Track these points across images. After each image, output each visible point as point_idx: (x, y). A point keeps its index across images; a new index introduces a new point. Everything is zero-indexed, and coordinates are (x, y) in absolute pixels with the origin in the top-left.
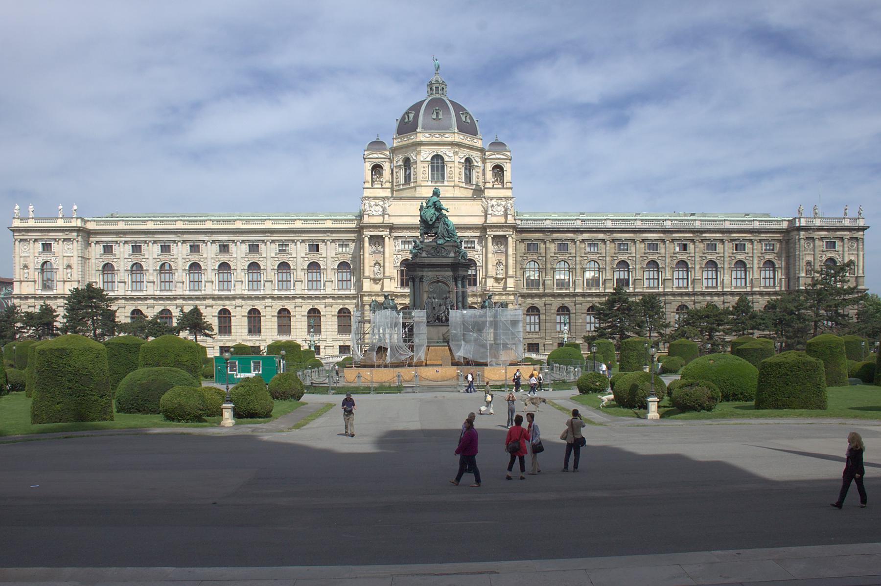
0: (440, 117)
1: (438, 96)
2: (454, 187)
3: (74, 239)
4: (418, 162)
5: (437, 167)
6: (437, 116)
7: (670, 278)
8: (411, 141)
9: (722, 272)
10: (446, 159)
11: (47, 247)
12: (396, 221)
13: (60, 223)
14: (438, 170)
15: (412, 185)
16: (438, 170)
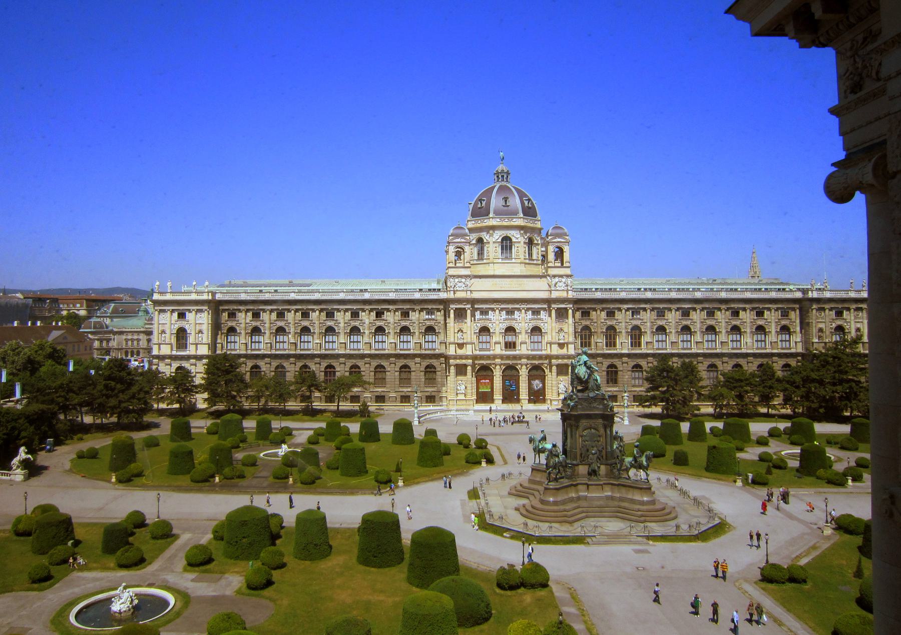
0: (508, 204)
1: (504, 183)
2: (521, 263)
3: (206, 310)
4: (491, 243)
5: (506, 246)
6: (506, 203)
7: (701, 341)
8: (484, 224)
9: (745, 335)
10: (514, 240)
11: (182, 315)
12: (476, 295)
13: (194, 297)
14: (506, 249)
15: (485, 261)
16: (506, 249)
